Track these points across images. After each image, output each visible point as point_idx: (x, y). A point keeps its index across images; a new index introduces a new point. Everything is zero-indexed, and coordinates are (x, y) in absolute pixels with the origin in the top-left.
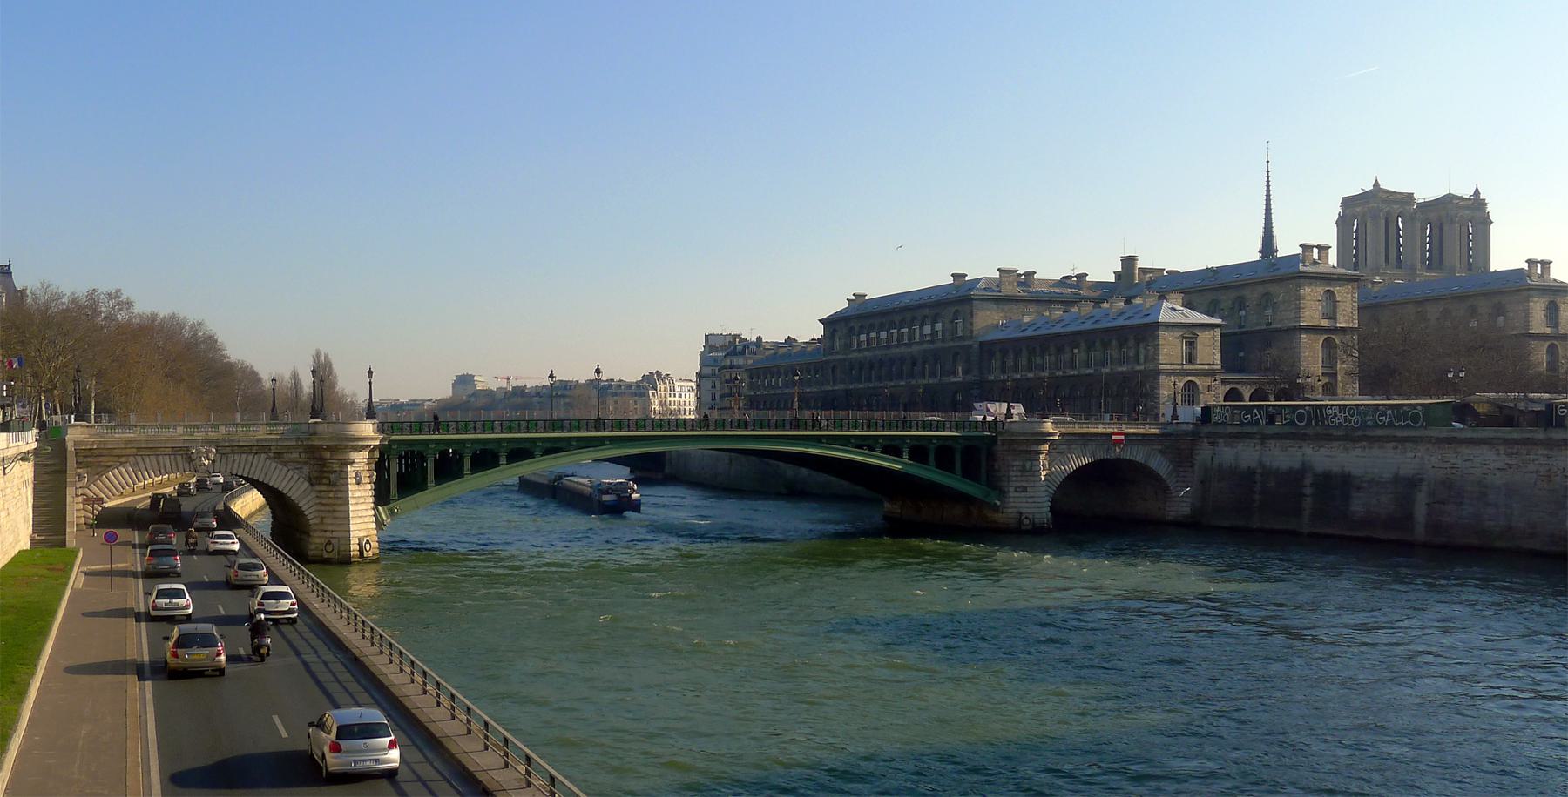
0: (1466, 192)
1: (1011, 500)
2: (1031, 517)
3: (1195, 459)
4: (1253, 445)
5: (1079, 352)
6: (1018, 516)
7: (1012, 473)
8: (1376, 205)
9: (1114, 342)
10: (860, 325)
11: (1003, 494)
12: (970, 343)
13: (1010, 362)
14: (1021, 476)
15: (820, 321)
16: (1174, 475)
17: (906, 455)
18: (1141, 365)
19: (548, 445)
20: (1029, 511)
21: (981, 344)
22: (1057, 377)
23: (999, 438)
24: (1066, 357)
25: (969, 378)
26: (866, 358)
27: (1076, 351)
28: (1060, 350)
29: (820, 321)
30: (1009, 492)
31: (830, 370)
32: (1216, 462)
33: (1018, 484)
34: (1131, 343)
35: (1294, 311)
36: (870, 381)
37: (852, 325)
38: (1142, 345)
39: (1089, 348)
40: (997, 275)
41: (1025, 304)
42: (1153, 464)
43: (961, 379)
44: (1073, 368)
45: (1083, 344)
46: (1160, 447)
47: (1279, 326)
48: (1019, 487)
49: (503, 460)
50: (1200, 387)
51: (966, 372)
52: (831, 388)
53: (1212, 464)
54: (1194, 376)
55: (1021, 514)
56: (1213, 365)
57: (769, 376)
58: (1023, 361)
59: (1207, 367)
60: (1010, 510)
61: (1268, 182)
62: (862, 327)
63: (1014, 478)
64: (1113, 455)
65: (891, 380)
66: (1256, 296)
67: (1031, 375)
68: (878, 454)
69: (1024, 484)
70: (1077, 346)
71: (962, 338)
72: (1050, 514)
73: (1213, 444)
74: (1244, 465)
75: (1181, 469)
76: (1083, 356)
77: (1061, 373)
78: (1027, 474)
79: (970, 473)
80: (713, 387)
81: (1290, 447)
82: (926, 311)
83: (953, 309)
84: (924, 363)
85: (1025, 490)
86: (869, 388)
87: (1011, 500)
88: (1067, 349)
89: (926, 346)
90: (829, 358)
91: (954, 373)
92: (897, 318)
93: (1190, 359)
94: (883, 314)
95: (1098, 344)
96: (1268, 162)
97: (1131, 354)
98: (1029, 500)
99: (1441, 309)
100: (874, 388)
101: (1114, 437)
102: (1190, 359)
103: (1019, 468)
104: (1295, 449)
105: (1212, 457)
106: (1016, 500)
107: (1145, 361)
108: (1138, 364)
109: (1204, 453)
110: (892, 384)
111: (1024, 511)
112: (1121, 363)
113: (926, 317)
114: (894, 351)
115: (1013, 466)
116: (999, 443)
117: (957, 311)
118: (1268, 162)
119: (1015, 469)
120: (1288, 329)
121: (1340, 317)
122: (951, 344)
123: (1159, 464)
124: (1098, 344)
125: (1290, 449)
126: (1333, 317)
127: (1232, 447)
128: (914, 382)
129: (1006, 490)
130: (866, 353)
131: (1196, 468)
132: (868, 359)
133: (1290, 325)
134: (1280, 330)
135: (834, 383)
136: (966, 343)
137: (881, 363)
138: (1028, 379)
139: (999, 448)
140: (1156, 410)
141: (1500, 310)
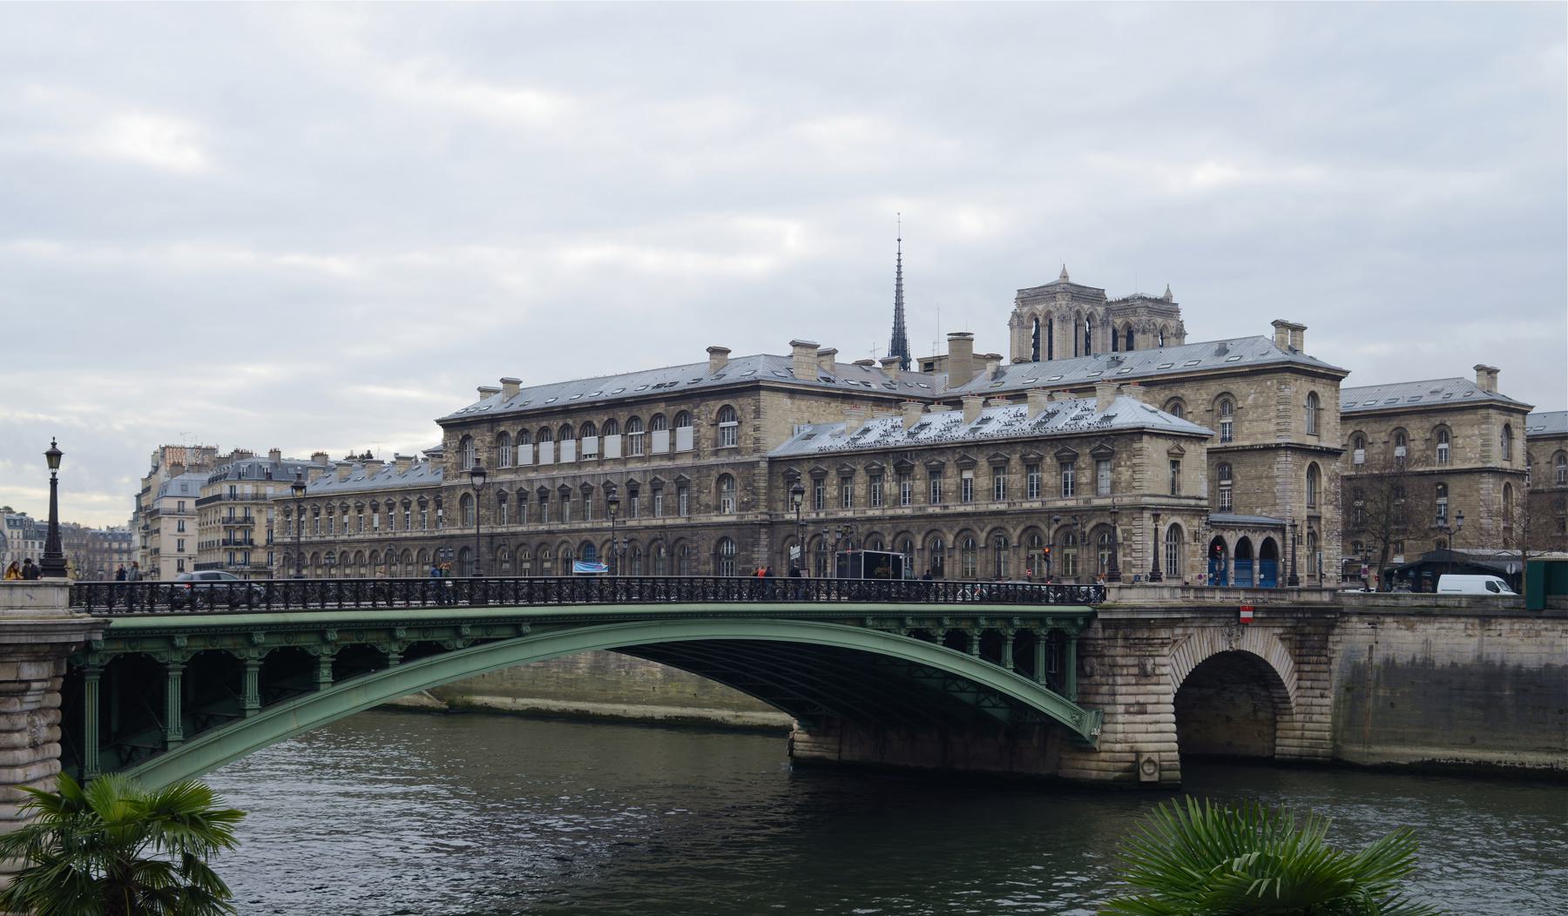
0: (1160, 294)
1: (1120, 728)
2: (1155, 757)
3: (1334, 652)
4: (1462, 626)
5: (975, 474)
6: (1132, 757)
7: (1119, 680)
8: (1064, 303)
9: (1049, 460)
10: (519, 428)
11: (1104, 719)
12: (755, 458)
13: (831, 490)
14: (1136, 684)
15: (438, 422)
16: (1296, 675)
17: (976, 649)
18: (1106, 497)
19: (415, 637)
20: (1152, 747)
21: (773, 461)
22: (931, 516)
23: (1100, 616)
24: (949, 482)
25: (750, 517)
26: (531, 481)
27: (967, 475)
28: (936, 472)
29: (438, 422)
30: (1114, 714)
31: (456, 503)
32: (1378, 658)
33: (1132, 699)
34: (1085, 461)
35: (1274, 421)
36: (540, 520)
37: (502, 429)
38: (1103, 466)
39: (999, 467)
40: (790, 350)
41: (828, 400)
42: (1273, 662)
43: (733, 519)
44: (964, 500)
45: (983, 462)
46: (1281, 631)
47: (1247, 443)
48: (1132, 705)
49: (325, 674)
50: (1186, 534)
51: (744, 507)
52: (458, 532)
53: (1370, 658)
54: (1179, 515)
55: (1138, 753)
56: (1200, 499)
57: (323, 511)
58: (860, 487)
59: (1193, 502)
60: (1118, 747)
61: (899, 266)
62: (524, 432)
63: (1124, 689)
64: (1234, 645)
65: (585, 519)
66: (1205, 396)
67: (877, 512)
68: (940, 647)
69: (1141, 699)
70: (972, 465)
71: (737, 451)
72: (1176, 755)
73: (1373, 625)
74: (1442, 660)
75: (1308, 668)
76: (983, 482)
77: (938, 510)
78: (1144, 681)
79: (1056, 683)
80: (181, 530)
81: (1546, 629)
82: (660, 408)
83: (716, 405)
84: (654, 491)
85: (1142, 709)
86: (538, 533)
87: (1120, 728)
88: (951, 470)
89: (656, 464)
90: (456, 482)
91: (719, 508)
92: (598, 420)
93: (1174, 486)
94: (566, 410)
95: (1015, 459)
96: (899, 240)
97: (1084, 480)
98: (1152, 728)
99: (1351, 431)
100: (549, 532)
101: (1244, 614)
102: (1174, 486)
103: (1135, 671)
104: (1555, 633)
105: (1371, 648)
106: (1128, 728)
107: (1112, 492)
108: (1098, 495)
109: (1354, 640)
110: (589, 525)
111: (1144, 747)
112: (1028, 493)
113: (659, 416)
114: (589, 470)
115: (1123, 666)
116: (1097, 625)
117: (727, 408)
118: (899, 240)
119: (1125, 672)
120: (1267, 449)
121: (1324, 432)
122: (713, 460)
123: (1279, 659)
124: (1015, 459)
125: (1543, 633)
126: (1315, 430)
127: (1411, 628)
128: (631, 523)
129: (1108, 709)
130: (532, 475)
131: (1335, 666)
132: (537, 486)
133: (1267, 442)
134: (1251, 450)
135: (464, 526)
136: (747, 459)
137: (565, 493)
138: (870, 520)
139: (1097, 631)
140: (1134, 570)
141: (1443, 434)
